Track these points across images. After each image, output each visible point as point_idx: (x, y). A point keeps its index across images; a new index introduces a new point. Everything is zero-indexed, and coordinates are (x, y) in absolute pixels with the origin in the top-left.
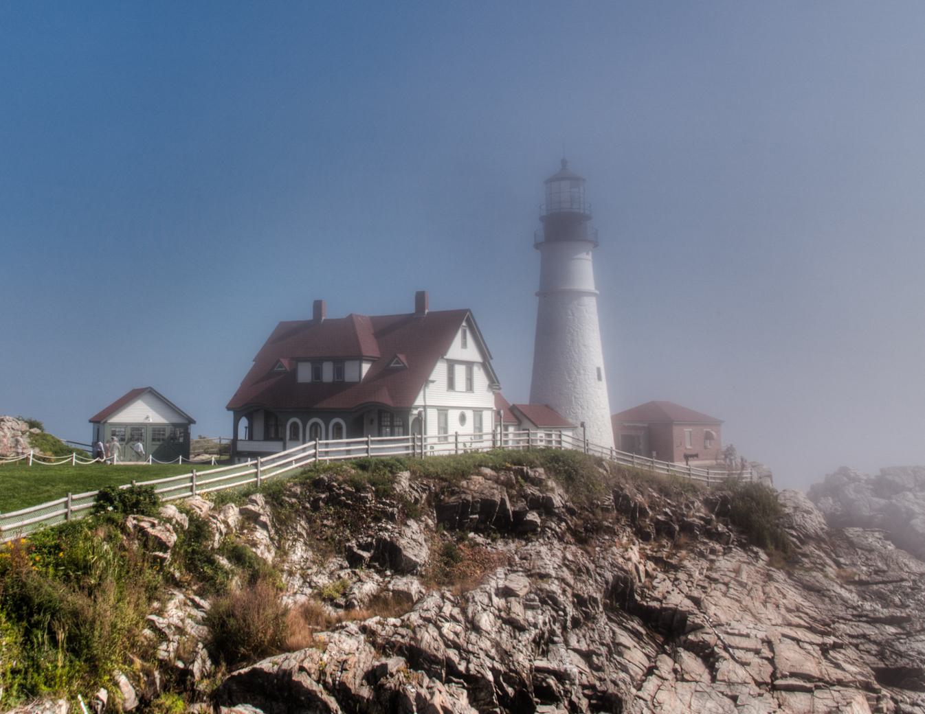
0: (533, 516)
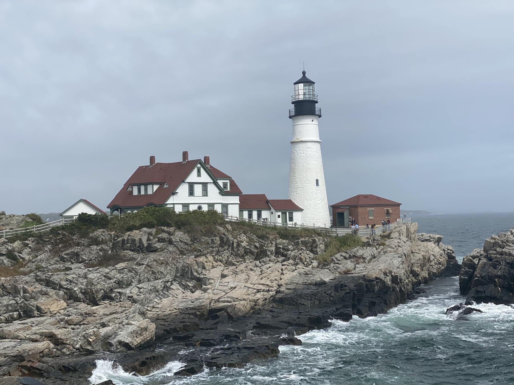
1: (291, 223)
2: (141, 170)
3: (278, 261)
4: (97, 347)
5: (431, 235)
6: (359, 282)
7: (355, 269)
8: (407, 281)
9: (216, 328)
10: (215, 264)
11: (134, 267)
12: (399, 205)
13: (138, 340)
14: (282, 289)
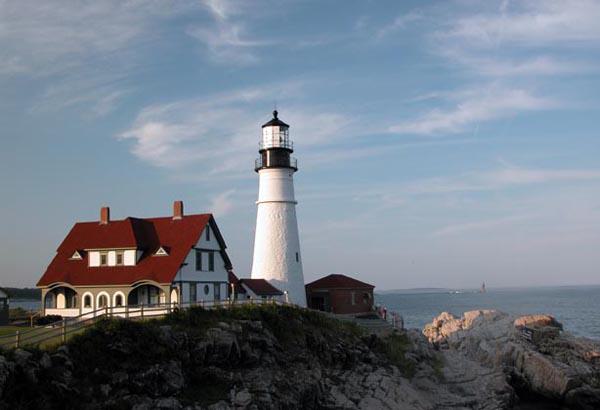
0: (256, 354)
12: (371, 288)
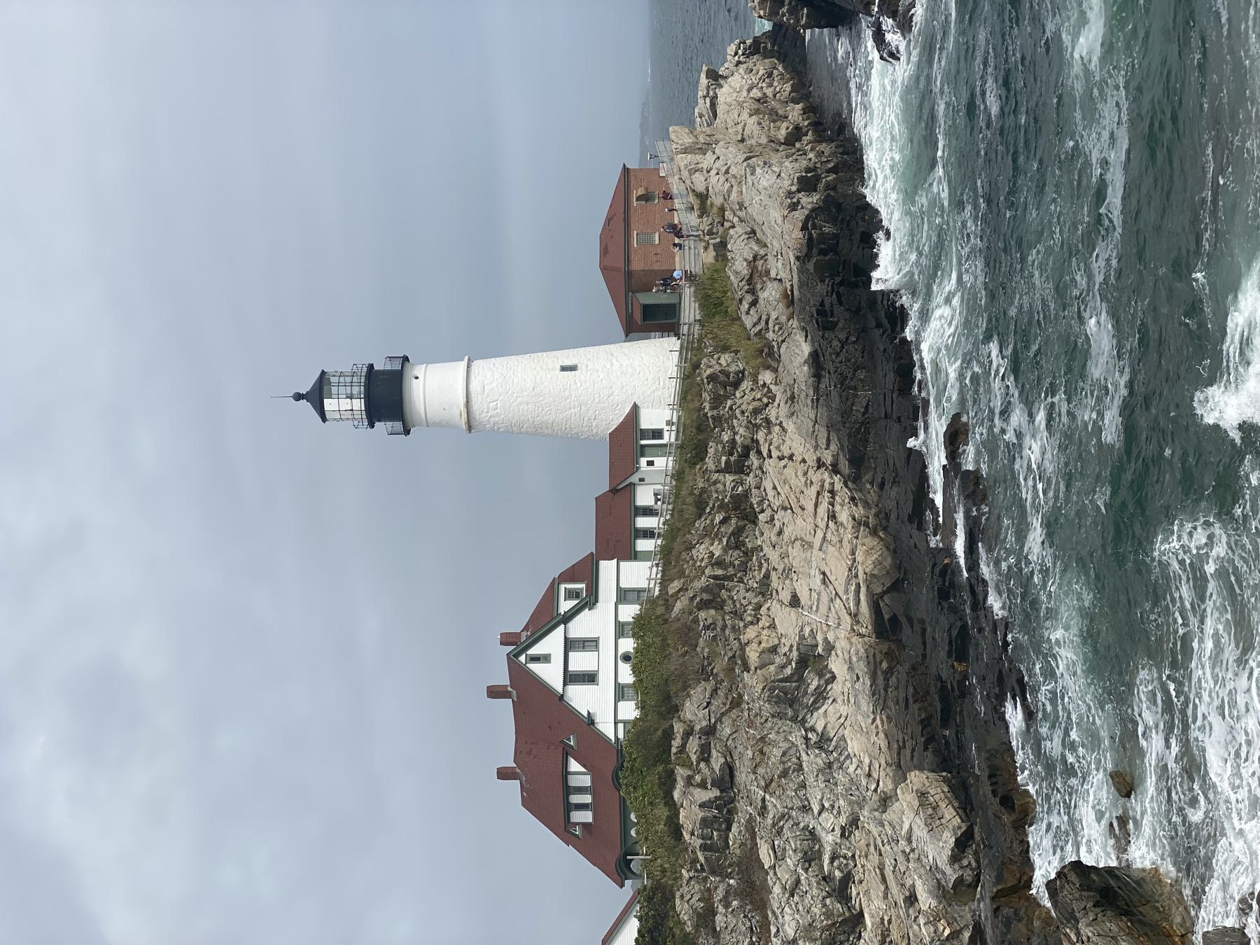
1: (666, 435)
2: (531, 802)
3: (761, 468)
4: (965, 915)
5: (700, 94)
6: (812, 270)
7: (780, 280)
8: (811, 153)
9: (922, 622)
10: (764, 622)
11: (770, 821)
12: (626, 171)
13: (949, 813)
14: (828, 458)
